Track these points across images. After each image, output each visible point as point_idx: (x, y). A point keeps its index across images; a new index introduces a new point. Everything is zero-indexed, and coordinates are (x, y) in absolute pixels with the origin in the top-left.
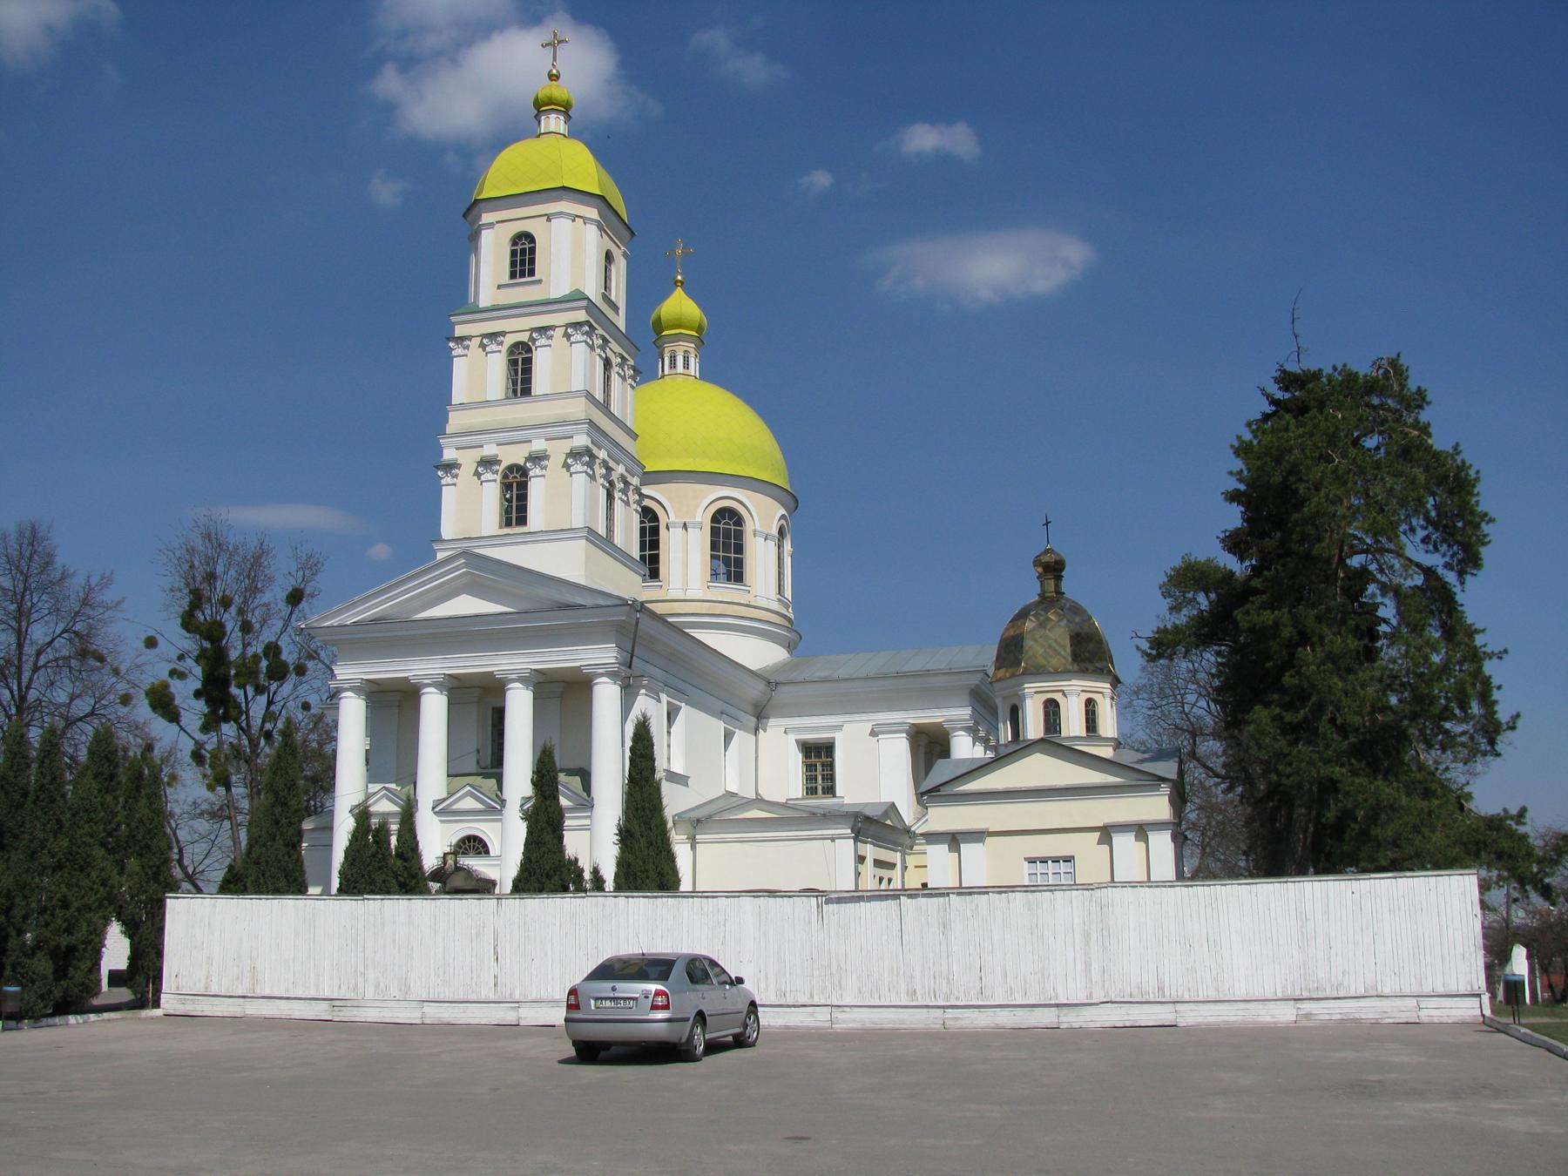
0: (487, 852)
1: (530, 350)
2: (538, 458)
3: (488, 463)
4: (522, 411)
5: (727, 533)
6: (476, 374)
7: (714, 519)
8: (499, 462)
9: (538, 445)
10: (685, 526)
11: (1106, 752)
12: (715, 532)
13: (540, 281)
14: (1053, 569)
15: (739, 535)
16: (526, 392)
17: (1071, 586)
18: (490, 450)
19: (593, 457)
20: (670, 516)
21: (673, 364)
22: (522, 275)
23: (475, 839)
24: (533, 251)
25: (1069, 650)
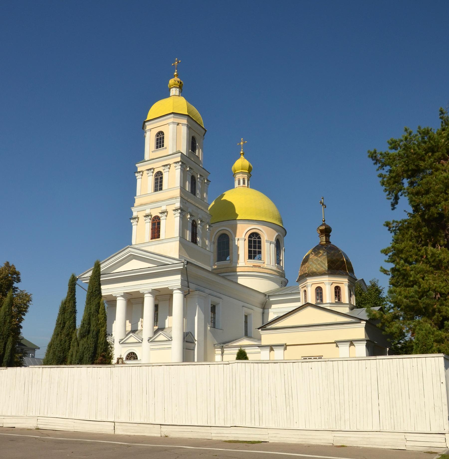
0: (137, 358)
1: (162, 174)
2: (162, 213)
3: (146, 216)
4: (160, 195)
5: (255, 242)
6: (144, 183)
7: (250, 237)
8: (151, 216)
9: (164, 208)
11: (346, 310)
12: (250, 242)
13: (166, 148)
14: (326, 232)
15: (260, 242)
17: (334, 240)
18: (148, 212)
21: (239, 184)
22: (160, 147)
23: (134, 353)
24: (163, 138)
25: (327, 265)
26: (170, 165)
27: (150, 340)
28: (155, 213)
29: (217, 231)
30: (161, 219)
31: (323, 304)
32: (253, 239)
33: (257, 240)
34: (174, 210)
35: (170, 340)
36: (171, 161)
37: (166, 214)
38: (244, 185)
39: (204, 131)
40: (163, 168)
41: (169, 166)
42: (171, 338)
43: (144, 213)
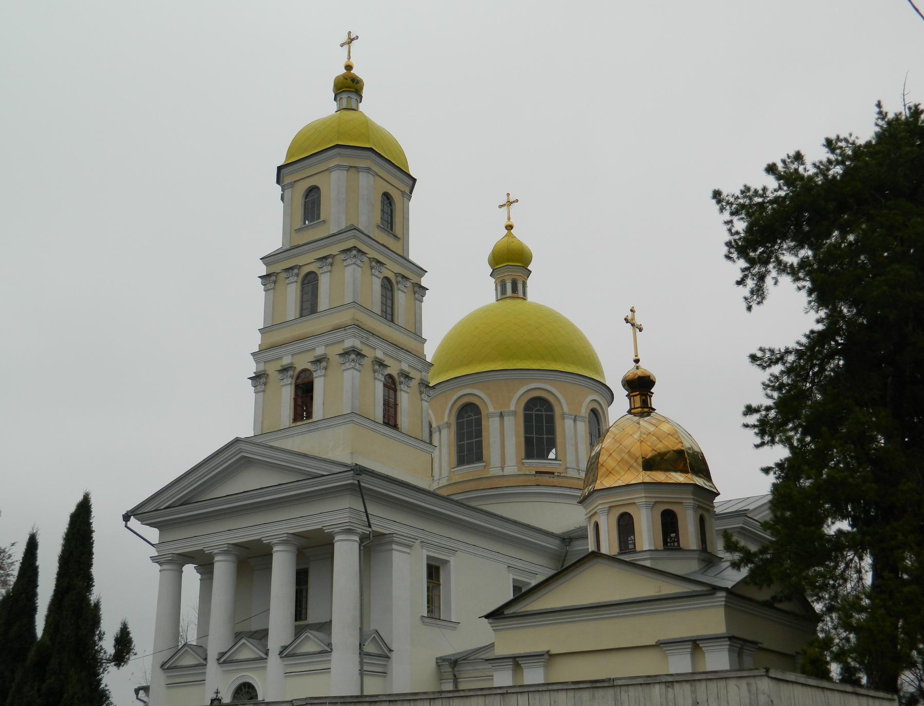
2: (318, 361)
3: (284, 370)
4: (312, 325)
5: (539, 417)
9: (320, 351)
10: (501, 415)
12: (527, 419)
13: (324, 221)
16: (313, 309)
18: (286, 361)
19: (359, 354)
20: (489, 407)
26: (333, 256)
27: (286, 653)
28: (302, 363)
29: (455, 397)
30: (315, 375)
31: (634, 551)
32: (534, 413)
33: (544, 413)
34: (341, 355)
35: (327, 650)
36: (334, 250)
37: (324, 364)
38: (515, 295)
39: (411, 182)
40: (318, 264)
41: (330, 260)
42: (330, 645)
43: (278, 365)
